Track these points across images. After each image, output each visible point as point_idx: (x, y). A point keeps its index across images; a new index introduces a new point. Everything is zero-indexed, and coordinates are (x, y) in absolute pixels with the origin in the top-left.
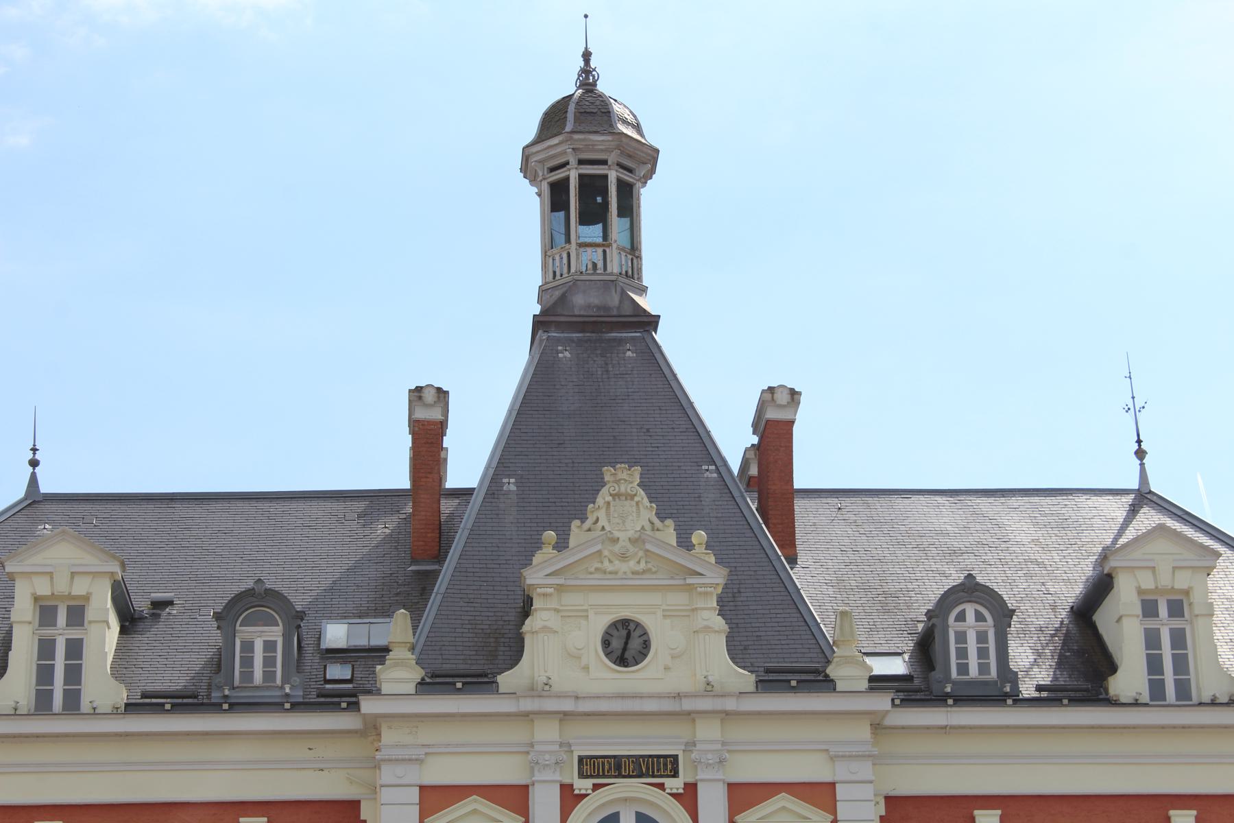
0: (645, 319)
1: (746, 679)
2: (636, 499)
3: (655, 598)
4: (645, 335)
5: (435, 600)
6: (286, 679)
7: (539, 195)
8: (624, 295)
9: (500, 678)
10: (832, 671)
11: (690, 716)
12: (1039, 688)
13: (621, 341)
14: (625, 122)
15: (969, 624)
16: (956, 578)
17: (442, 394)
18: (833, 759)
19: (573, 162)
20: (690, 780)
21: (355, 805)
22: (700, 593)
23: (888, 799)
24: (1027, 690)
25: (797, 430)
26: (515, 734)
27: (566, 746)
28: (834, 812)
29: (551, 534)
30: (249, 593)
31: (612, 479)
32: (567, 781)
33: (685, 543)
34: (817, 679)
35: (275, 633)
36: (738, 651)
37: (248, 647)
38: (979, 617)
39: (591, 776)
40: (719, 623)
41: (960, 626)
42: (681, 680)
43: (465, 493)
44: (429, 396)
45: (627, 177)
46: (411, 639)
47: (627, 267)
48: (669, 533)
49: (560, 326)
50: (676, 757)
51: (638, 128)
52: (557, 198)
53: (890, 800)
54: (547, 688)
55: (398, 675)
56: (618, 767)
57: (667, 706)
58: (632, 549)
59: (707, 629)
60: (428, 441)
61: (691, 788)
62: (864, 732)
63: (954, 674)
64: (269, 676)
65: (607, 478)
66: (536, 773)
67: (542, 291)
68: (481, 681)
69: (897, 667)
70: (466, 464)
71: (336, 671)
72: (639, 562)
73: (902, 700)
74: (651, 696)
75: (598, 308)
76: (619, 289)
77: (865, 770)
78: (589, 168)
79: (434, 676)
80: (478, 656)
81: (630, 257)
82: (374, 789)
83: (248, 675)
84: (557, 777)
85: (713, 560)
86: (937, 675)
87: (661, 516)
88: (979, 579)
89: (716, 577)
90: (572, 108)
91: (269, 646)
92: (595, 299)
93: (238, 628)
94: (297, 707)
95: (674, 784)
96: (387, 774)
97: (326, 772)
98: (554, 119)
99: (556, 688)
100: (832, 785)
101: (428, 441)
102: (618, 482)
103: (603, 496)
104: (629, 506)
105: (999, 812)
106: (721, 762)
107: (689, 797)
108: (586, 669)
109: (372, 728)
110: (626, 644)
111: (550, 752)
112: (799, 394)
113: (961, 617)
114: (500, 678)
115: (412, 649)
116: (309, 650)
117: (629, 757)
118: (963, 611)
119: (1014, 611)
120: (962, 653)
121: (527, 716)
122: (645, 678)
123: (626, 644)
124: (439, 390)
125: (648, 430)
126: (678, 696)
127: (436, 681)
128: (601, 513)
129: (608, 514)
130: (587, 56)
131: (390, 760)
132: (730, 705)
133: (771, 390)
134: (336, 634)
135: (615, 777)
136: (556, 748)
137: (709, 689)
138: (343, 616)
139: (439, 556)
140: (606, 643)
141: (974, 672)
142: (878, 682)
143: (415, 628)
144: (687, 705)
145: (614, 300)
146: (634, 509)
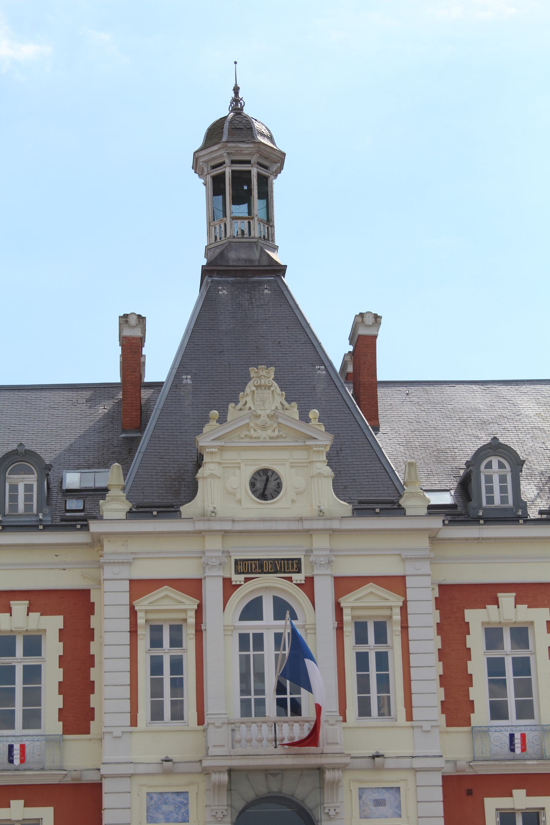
0: (277, 268)
1: (346, 508)
2: (272, 389)
3: (285, 455)
4: (277, 279)
5: (138, 457)
6: (39, 510)
7: (205, 184)
8: (262, 252)
9: (182, 508)
10: (403, 502)
11: (309, 532)
12: (541, 512)
13: (261, 283)
14: (262, 134)
15: (495, 470)
16: (486, 440)
17: (141, 319)
18: (404, 560)
19: (228, 162)
20: (309, 575)
21: (86, 592)
22: (315, 451)
23: (441, 586)
24: (533, 513)
25: (378, 341)
26: (193, 545)
27: (227, 553)
28: (405, 595)
29: (215, 413)
30: (14, 453)
31: (255, 375)
32: (227, 576)
33: (304, 418)
34: (394, 508)
35: (32, 479)
36: (340, 490)
37: (14, 488)
38: (501, 465)
39: (243, 573)
40: (328, 471)
41: (488, 472)
42: (302, 509)
43: (157, 385)
44: (133, 321)
45: (263, 172)
46: (122, 483)
47: (264, 232)
48: (294, 411)
49: (221, 273)
50: (299, 560)
51: (271, 138)
52: (217, 186)
53: (442, 587)
54: (213, 514)
55: (115, 507)
56: (261, 566)
57: (294, 526)
58: (269, 422)
59: (320, 475)
60: (132, 350)
61: (310, 580)
62: (425, 542)
63: (484, 503)
64: (28, 507)
65: (252, 375)
66: (207, 570)
67: (208, 249)
68: (170, 510)
69: (446, 499)
70: (158, 365)
71: (74, 504)
72: (274, 431)
73: (450, 521)
74: (282, 520)
75: (246, 261)
76: (259, 248)
77: (425, 567)
78: (239, 166)
79: (138, 507)
80: (166, 495)
81: (266, 226)
82: (99, 582)
83: (14, 507)
84: (221, 573)
85: (323, 429)
86: (473, 504)
87: (289, 400)
88: (501, 440)
89: (325, 441)
90: (226, 125)
91: (28, 488)
92: (243, 256)
93: (7, 476)
94: (47, 528)
95: (299, 578)
96: (108, 572)
97: (67, 570)
98: (214, 133)
99: (220, 514)
100: (404, 577)
101: (132, 350)
102: (259, 377)
103: (250, 387)
104: (267, 393)
105: (514, 594)
106: (330, 562)
107: (308, 586)
108: (240, 501)
109: (97, 542)
110: (266, 485)
111: (215, 557)
112: (381, 317)
113: (489, 466)
114: (182, 508)
115: (124, 489)
116: (55, 490)
117: (268, 560)
118: (491, 461)
119: (524, 461)
120: (490, 490)
121: (200, 533)
122: (280, 507)
123: (266, 485)
124: (139, 316)
125: (279, 343)
126: (301, 519)
127: (139, 511)
128: (249, 399)
129: (253, 399)
130: (236, 90)
131: (109, 563)
132: (336, 525)
133: (361, 315)
134: (72, 479)
135: (260, 573)
136: (220, 554)
137: (321, 515)
138: (77, 468)
139: (141, 428)
140: (252, 485)
141: (497, 502)
142: (434, 510)
143: (125, 475)
144: (307, 525)
145: (256, 255)
146: (271, 395)
